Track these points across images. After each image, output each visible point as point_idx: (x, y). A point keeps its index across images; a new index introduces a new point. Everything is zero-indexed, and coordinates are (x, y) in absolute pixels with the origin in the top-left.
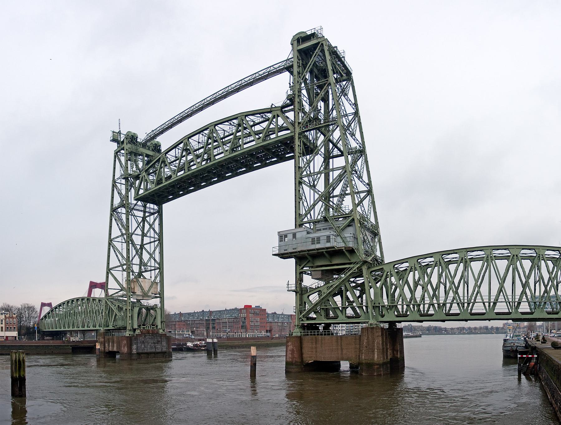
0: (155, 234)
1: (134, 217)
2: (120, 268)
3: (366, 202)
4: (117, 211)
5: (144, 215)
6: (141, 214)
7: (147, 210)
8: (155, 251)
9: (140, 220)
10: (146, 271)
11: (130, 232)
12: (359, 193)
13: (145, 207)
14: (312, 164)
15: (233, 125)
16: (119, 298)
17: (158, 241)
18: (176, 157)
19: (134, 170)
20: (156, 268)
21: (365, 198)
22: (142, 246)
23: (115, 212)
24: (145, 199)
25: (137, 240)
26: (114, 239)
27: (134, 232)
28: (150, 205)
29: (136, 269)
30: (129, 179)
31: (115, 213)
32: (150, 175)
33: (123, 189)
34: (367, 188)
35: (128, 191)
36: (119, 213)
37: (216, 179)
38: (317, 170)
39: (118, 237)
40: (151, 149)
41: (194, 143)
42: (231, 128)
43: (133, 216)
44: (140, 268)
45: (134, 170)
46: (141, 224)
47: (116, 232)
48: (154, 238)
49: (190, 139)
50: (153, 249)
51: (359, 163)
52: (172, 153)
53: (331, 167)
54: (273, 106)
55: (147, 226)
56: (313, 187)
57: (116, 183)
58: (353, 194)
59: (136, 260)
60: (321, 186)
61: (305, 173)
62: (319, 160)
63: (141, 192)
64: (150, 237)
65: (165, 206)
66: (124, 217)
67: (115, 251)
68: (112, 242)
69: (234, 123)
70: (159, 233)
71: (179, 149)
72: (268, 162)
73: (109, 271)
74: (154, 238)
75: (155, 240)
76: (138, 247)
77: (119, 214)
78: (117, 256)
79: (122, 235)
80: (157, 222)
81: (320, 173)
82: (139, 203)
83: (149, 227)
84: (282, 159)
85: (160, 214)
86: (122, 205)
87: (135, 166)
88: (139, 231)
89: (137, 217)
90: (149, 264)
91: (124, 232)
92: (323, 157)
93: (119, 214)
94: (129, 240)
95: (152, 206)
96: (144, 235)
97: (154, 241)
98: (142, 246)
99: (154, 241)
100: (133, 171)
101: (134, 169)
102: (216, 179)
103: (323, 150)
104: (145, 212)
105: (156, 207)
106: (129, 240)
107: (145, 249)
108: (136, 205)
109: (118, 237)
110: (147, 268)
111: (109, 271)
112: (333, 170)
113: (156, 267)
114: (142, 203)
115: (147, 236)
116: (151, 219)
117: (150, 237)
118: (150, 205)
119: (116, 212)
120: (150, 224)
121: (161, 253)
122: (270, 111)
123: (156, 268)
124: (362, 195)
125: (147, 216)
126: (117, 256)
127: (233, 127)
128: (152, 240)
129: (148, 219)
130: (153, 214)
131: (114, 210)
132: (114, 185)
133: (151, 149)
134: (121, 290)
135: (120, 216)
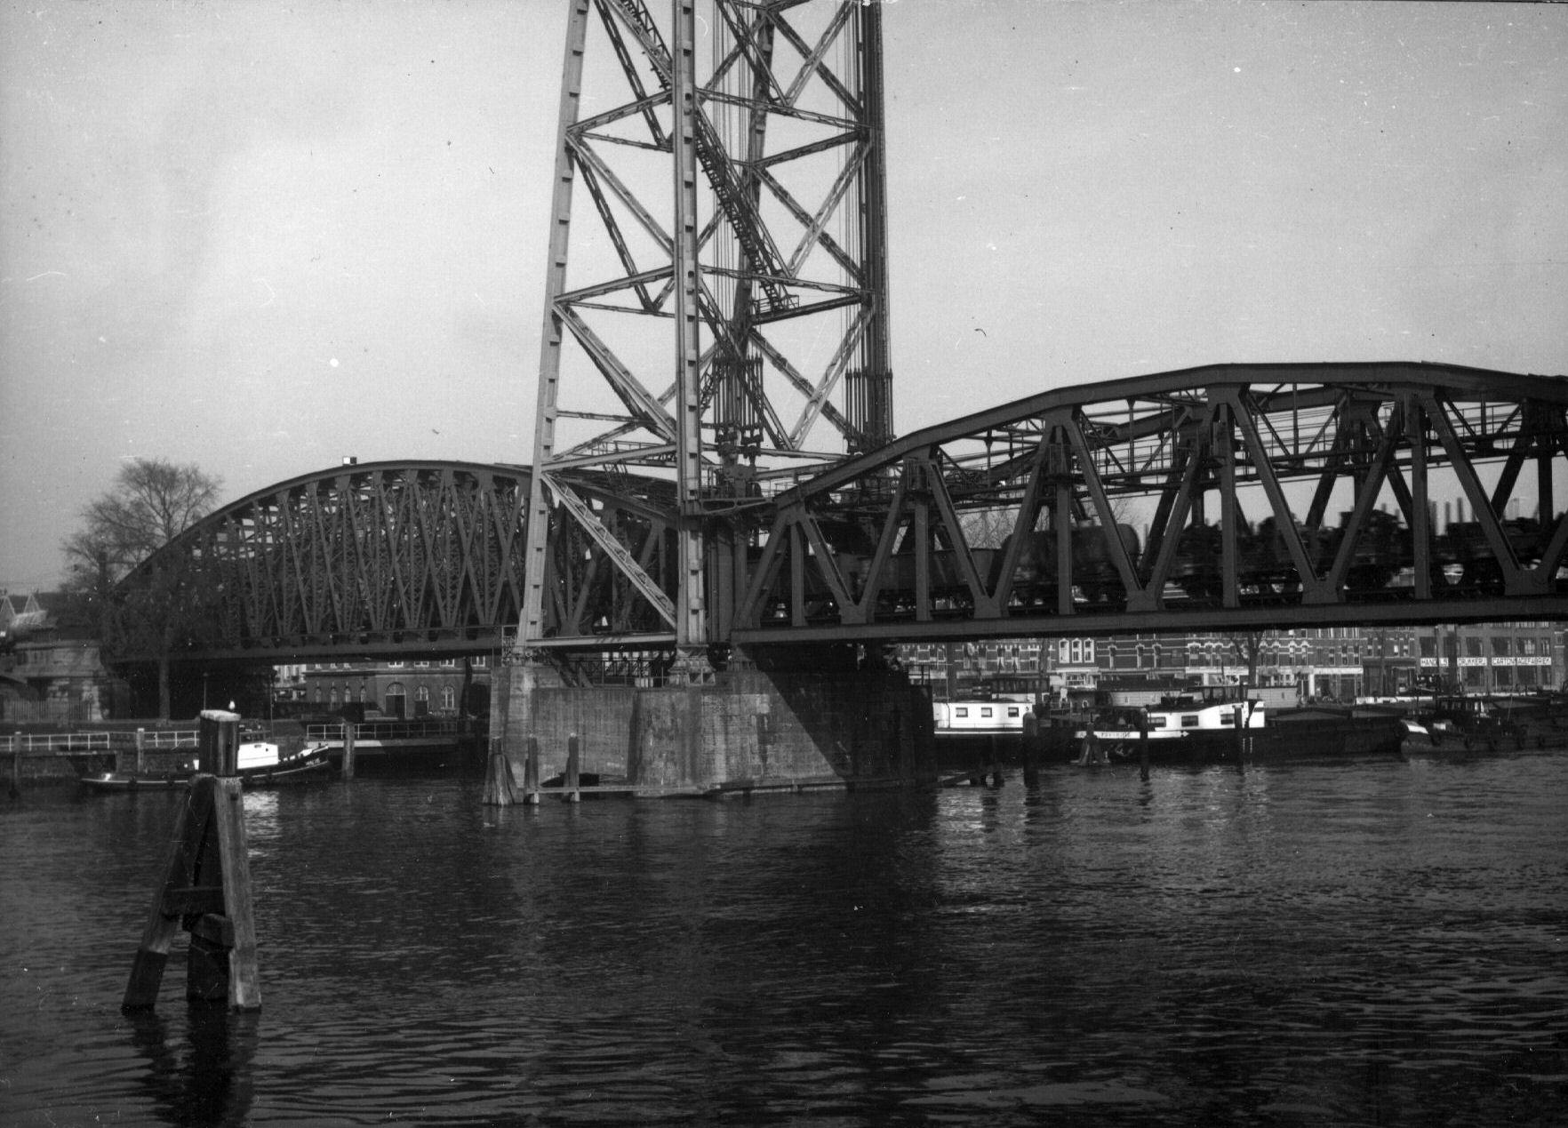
2: (629, 298)
10: (780, 312)
16: (621, 468)
26: (594, 122)
29: (723, 294)
39: (619, 113)
44: (743, 294)
59: (724, 249)
67: (597, 195)
68: (585, 139)
70: (859, 92)
73: (567, 309)
78: (610, 223)
79: (644, 103)
88: (738, 80)
91: (652, 85)
98: (757, 170)
109: (619, 113)
110: (788, 296)
111: (567, 309)
126: (610, 223)
134: (630, 426)
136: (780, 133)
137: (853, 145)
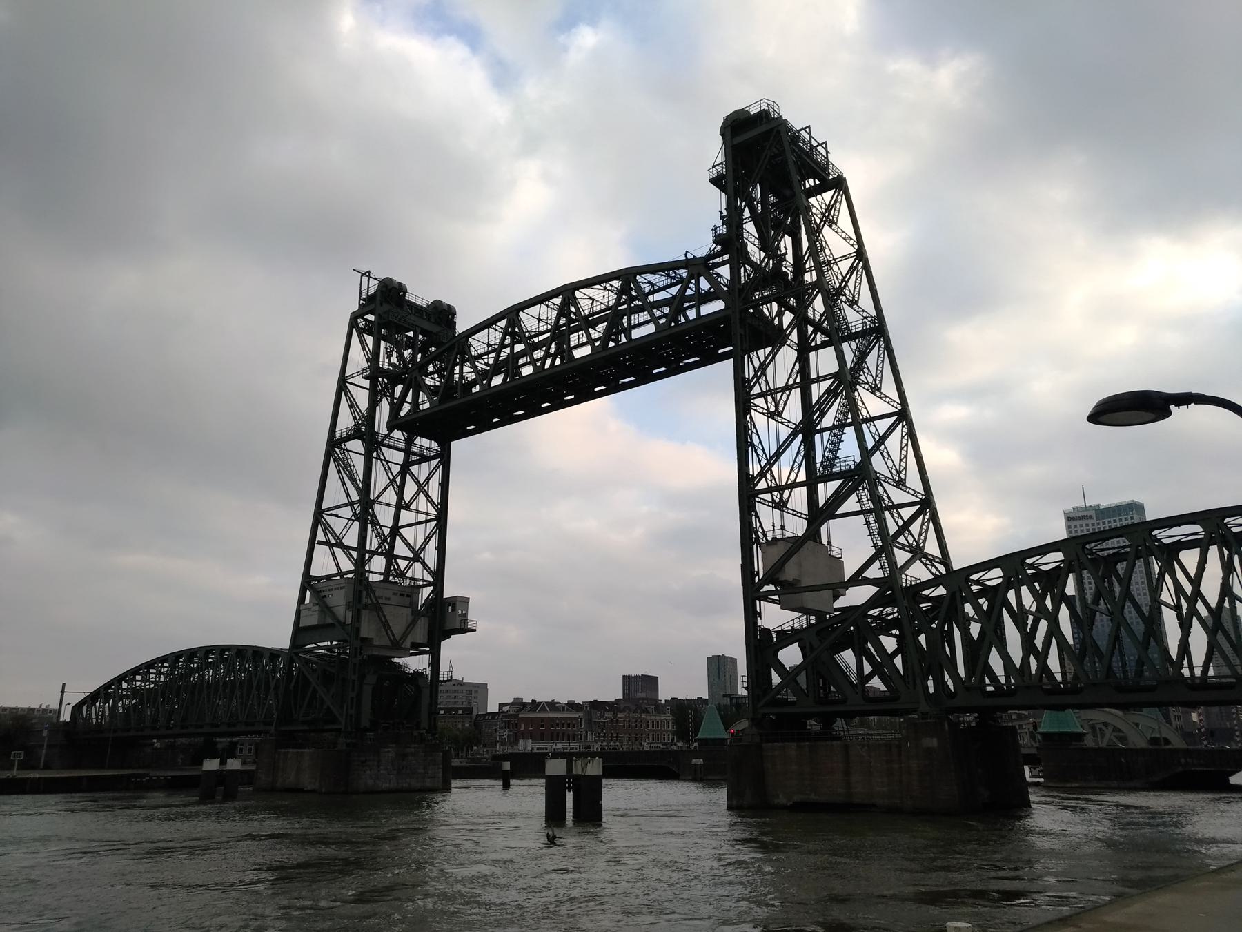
0: (429, 504)
1: (383, 465)
3: (894, 442)
4: (343, 446)
5: (406, 458)
6: (399, 457)
7: (414, 449)
8: (425, 541)
9: (396, 469)
11: (372, 498)
12: (872, 419)
13: (409, 442)
14: (769, 371)
15: (611, 290)
17: (435, 522)
18: (489, 345)
19: (392, 362)
20: (425, 583)
21: (891, 429)
22: (395, 530)
23: (338, 448)
24: (413, 426)
25: (385, 516)
26: (328, 509)
27: (379, 496)
28: (421, 441)
30: (380, 379)
31: (337, 450)
32: (428, 377)
33: (363, 399)
34: (896, 407)
35: (373, 403)
36: (348, 451)
37: (573, 397)
38: (781, 383)
39: (340, 507)
40: (433, 320)
41: (529, 321)
42: (606, 296)
43: (381, 460)
45: (392, 362)
46: (398, 480)
47: (335, 494)
48: (426, 513)
49: (521, 313)
50: (421, 540)
51: (871, 360)
52: (482, 336)
53: (813, 375)
54: (690, 256)
55: (410, 488)
56: (775, 415)
57: (347, 384)
58: (858, 425)
60: (793, 411)
61: (756, 390)
62: (787, 357)
63: (406, 408)
64: (417, 511)
65: (459, 448)
66: (358, 463)
68: (324, 515)
69: (611, 286)
71: (496, 330)
72: (681, 364)
74: (426, 513)
75: (429, 518)
76: (387, 531)
77: (346, 453)
80: (437, 479)
81: (788, 388)
82: (397, 434)
83: (415, 488)
84: (710, 358)
85: (444, 462)
86: (355, 434)
87: (395, 354)
88: (391, 496)
89: (389, 464)
90: (409, 575)
91: (355, 496)
92: (796, 350)
93: (346, 453)
94: (365, 514)
95: (426, 442)
96: (401, 505)
97: (426, 522)
98: (395, 530)
99: (426, 522)
100: (390, 364)
101: (394, 360)
102: (573, 397)
103: (794, 336)
104: (407, 452)
105: (435, 445)
106: (365, 514)
107: (402, 538)
108: (388, 436)
109: (340, 507)
112: (819, 379)
113: (426, 581)
114: (404, 435)
115: (410, 510)
116: (421, 470)
117: (417, 511)
118: (421, 441)
119: (341, 449)
120: (417, 483)
121: (441, 549)
122: (686, 263)
123: (425, 583)
124: (883, 425)
125: (414, 463)
127: (611, 294)
128: (422, 518)
129: (414, 469)
130: (429, 459)
131: (334, 444)
132: (343, 386)
133: (433, 320)
135: (349, 458)
136: (406, 517)
137: (435, 522)
